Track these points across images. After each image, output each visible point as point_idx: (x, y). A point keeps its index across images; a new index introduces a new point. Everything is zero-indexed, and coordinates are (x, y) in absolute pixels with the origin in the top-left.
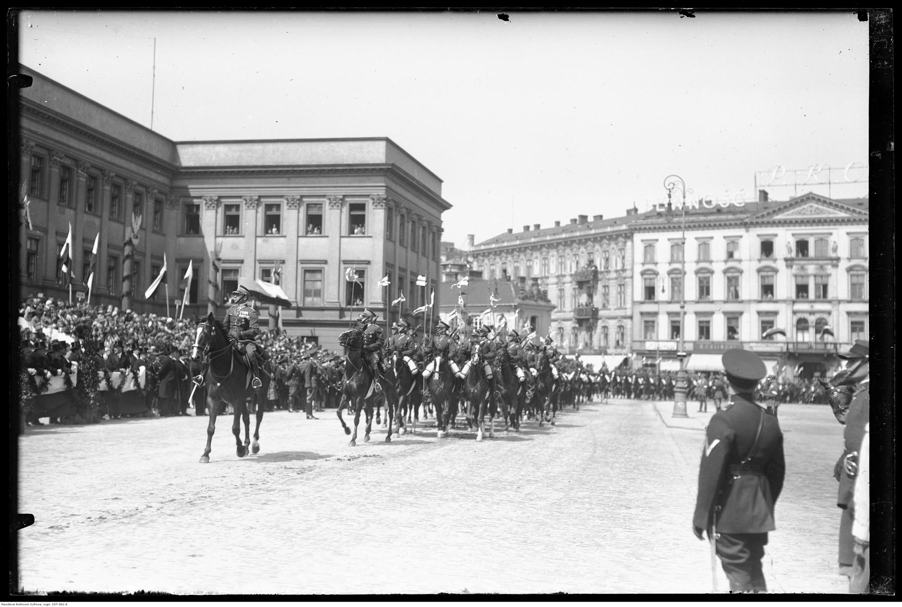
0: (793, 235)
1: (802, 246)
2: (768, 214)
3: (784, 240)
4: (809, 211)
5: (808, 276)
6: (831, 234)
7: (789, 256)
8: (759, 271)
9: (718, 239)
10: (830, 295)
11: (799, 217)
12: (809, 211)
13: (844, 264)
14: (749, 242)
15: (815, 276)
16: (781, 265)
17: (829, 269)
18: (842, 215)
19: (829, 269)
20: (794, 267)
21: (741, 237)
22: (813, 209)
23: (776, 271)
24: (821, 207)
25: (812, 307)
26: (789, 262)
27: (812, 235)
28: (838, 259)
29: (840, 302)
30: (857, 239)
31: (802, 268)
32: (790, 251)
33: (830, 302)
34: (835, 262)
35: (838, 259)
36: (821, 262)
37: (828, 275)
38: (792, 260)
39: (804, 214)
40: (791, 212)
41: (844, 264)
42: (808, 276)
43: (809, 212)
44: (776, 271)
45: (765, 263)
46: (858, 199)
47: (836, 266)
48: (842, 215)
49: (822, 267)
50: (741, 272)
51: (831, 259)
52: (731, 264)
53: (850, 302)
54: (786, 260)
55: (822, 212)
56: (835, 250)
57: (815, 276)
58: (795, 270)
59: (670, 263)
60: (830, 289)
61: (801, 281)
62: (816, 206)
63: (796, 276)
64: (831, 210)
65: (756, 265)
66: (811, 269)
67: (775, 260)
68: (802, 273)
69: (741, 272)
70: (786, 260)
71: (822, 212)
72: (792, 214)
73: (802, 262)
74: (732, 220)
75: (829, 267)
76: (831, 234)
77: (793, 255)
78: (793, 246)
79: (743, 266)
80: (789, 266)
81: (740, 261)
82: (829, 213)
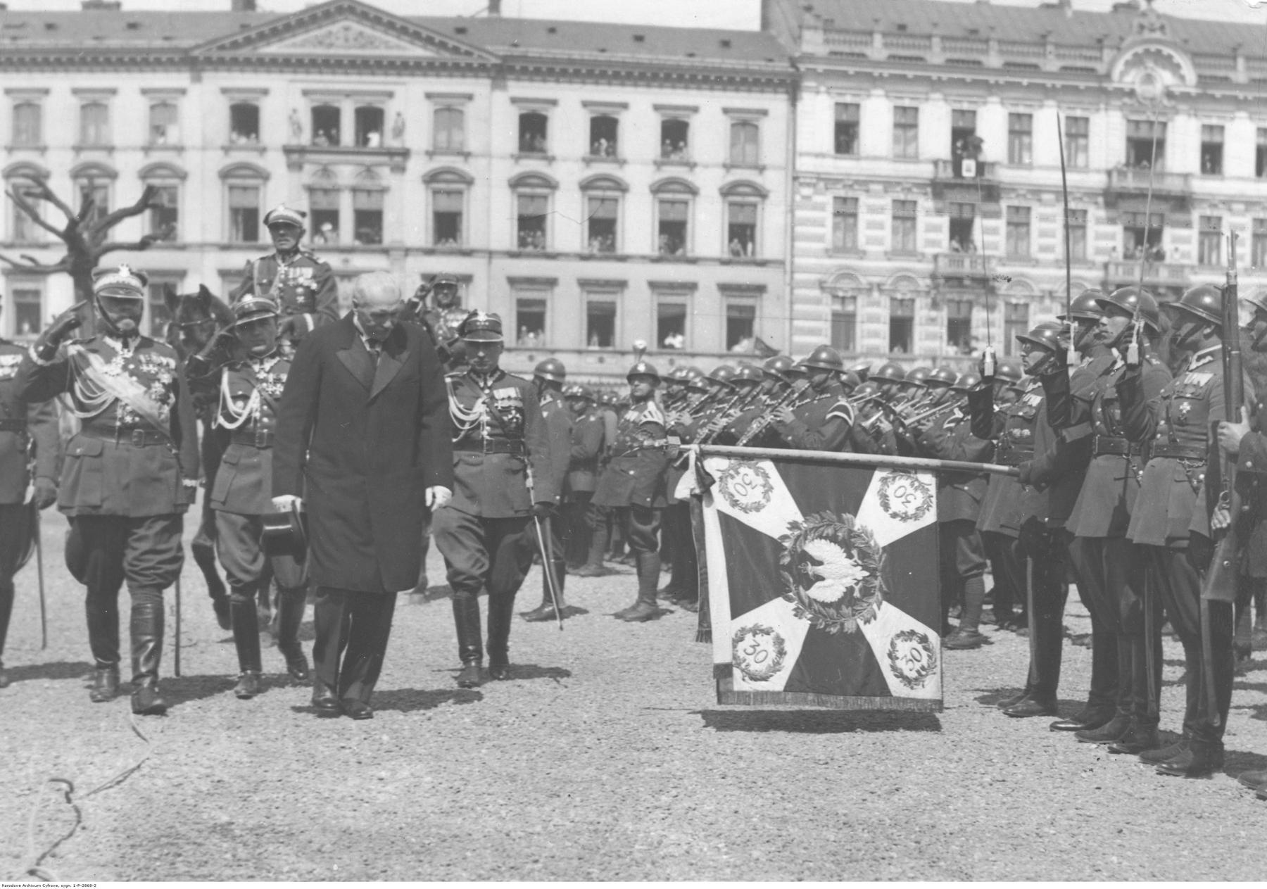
0: (306, 93)
1: (325, 119)
2: (248, 41)
3: (285, 103)
4: (342, 37)
5: (337, 190)
6: (390, 95)
7: (294, 142)
8: (225, 175)
9: (129, 93)
10: (390, 235)
11: (320, 51)
12: (342, 37)
13: (418, 166)
14: (203, 104)
15: (355, 190)
16: (275, 162)
17: (386, 176)
18: (416, 51)
19: (386, 176)
20: (308, 168)
21: (183, 92)
22: (351, 35)
23: (265, 176)
24: (368, 31)
25: (346, 261)
26: (295, 157)
27: (348, 94)
28: (405, 154)
29: (407, 251)
30: (449, 109)
31: (326, 171)
32: (298, 128)
33: (386, 252)
34: (398, 159)
35: (405, 154)
36: (368, 160)
37: (384, 191)
38: (302, 151)
39: (331, 45)
40: (300, 38)
41: (418, 166)
42: (337, 190)
43: (341, 42)
44: (265, 176)
45: (237, 157)
46: (460, 18)
47: (401, 169)
48: (416, 51)
49: (369, 171)
50: (183, 176)
51: (391, 153)
52: (156, 157)
53: (429, 252)
54: (288, 151)
55: (371, 43)
56: (399, 132)
57: (355, 190)
58: (308, 175)
59: (10, 150)
60: (389, 219)
61: (323, 203)
62: (356, 27)
63: (311, 190)
64: (392, 40)
65: (218, 161)
66: (346, 173)
67: (263, 150)
68: (325, 183)
69: (183, 176)
70: (288, 151)
71: (371, 43)
72: (303, 45)
73: (325, 158)
74: (162, 50)
75: (385, 171)
76: (390, 95)
77: (305, 138)
78: (306, 120)
79: (188, 162)
80: (295, 167)
81: (180, 149)
82: (398, 47)
